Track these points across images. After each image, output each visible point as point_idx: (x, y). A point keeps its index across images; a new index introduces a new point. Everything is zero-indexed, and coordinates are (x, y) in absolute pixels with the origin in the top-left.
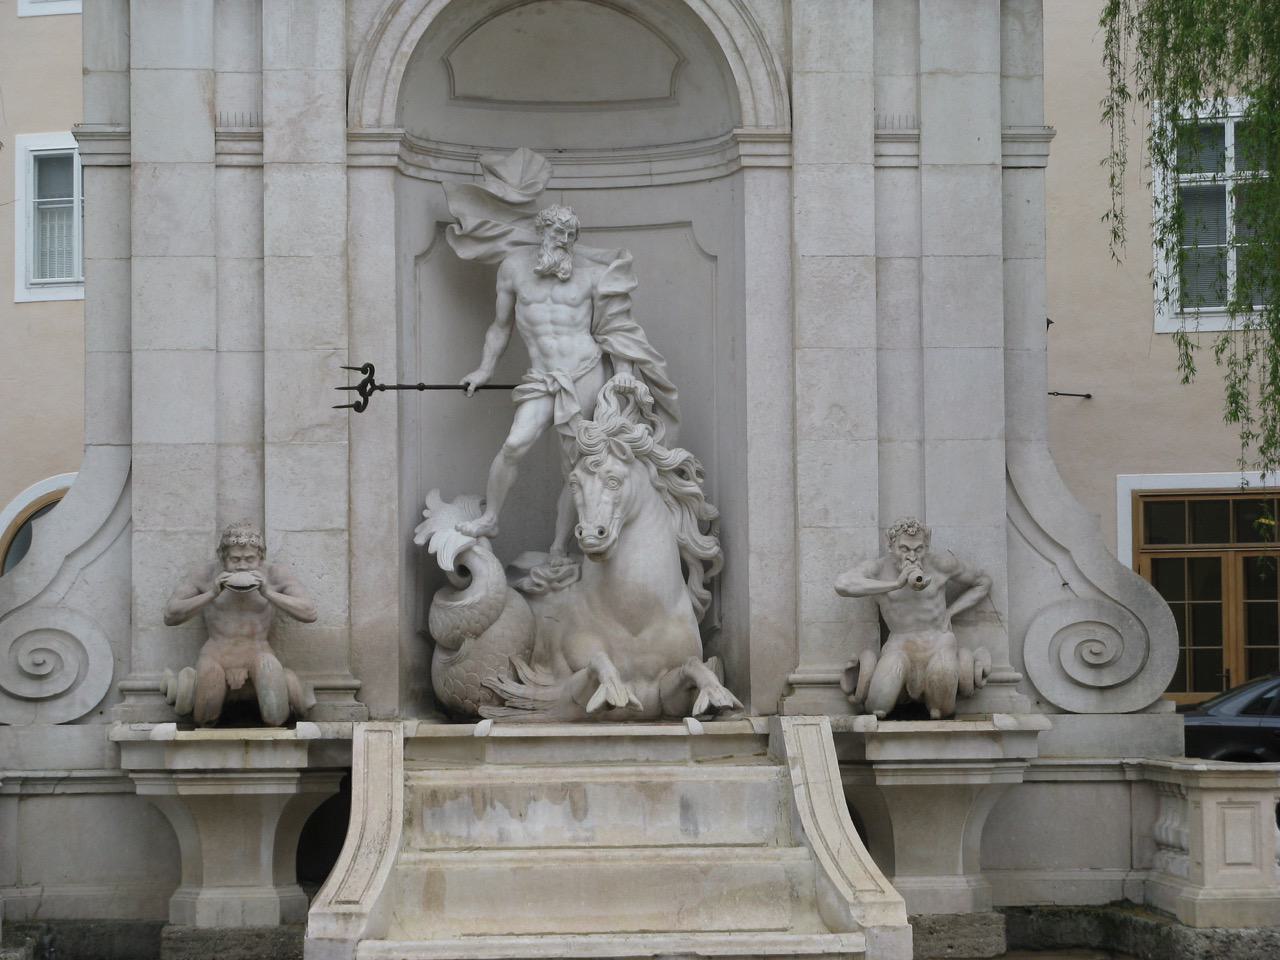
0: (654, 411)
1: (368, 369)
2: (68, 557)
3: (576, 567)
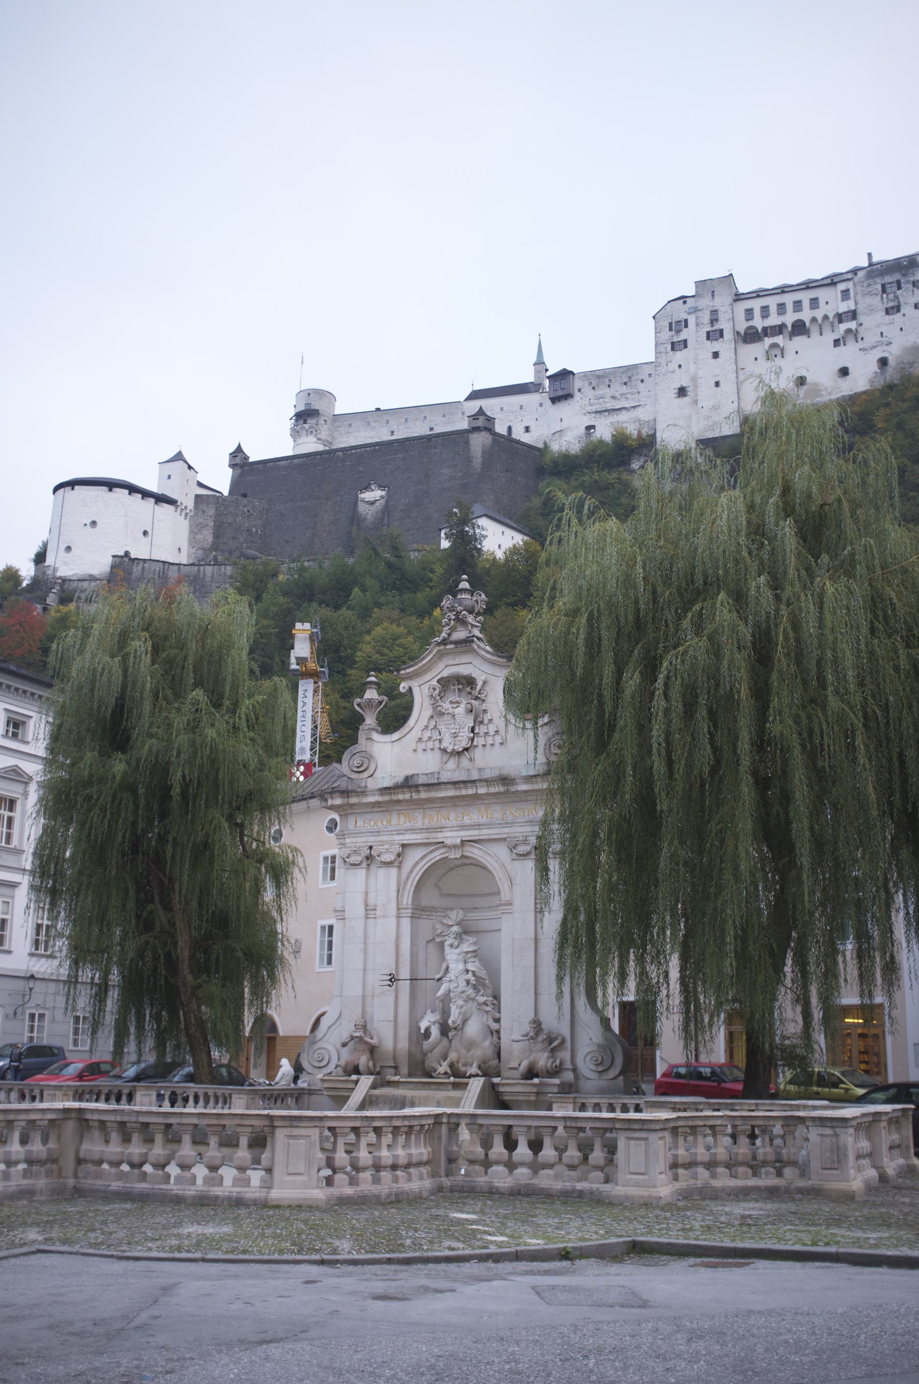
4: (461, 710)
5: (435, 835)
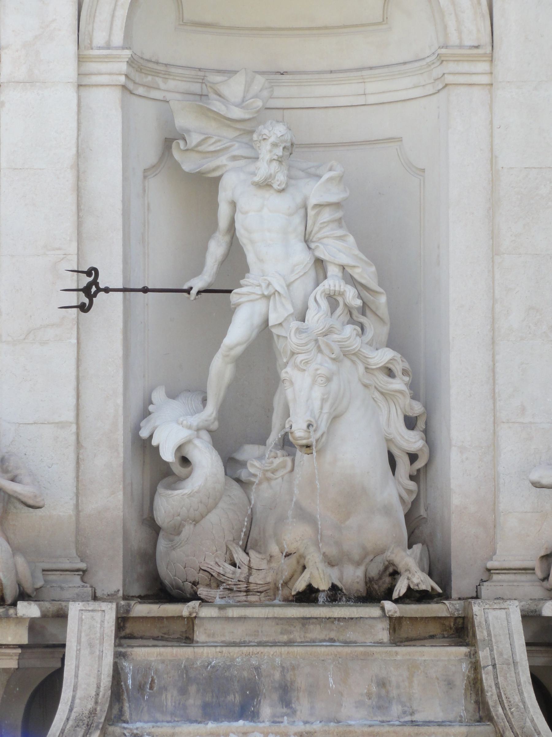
0: (364, 314)
1: (93, 272)
3: (289, 460)
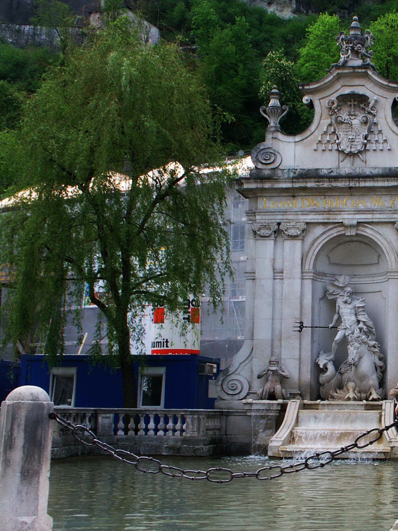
1: (301, 323)
2: (240, 364)
4: (356, 122)
5: (334, 216)
